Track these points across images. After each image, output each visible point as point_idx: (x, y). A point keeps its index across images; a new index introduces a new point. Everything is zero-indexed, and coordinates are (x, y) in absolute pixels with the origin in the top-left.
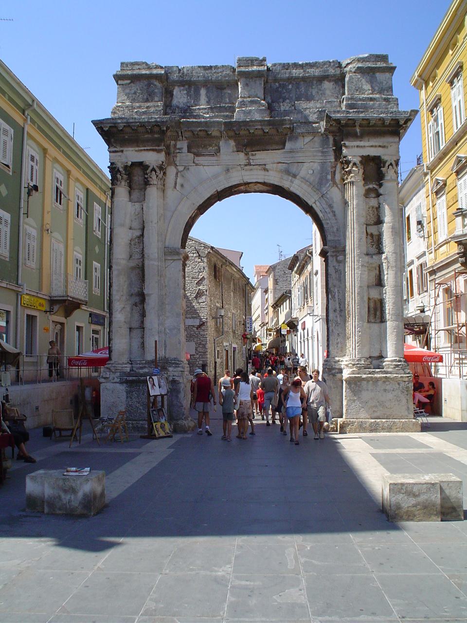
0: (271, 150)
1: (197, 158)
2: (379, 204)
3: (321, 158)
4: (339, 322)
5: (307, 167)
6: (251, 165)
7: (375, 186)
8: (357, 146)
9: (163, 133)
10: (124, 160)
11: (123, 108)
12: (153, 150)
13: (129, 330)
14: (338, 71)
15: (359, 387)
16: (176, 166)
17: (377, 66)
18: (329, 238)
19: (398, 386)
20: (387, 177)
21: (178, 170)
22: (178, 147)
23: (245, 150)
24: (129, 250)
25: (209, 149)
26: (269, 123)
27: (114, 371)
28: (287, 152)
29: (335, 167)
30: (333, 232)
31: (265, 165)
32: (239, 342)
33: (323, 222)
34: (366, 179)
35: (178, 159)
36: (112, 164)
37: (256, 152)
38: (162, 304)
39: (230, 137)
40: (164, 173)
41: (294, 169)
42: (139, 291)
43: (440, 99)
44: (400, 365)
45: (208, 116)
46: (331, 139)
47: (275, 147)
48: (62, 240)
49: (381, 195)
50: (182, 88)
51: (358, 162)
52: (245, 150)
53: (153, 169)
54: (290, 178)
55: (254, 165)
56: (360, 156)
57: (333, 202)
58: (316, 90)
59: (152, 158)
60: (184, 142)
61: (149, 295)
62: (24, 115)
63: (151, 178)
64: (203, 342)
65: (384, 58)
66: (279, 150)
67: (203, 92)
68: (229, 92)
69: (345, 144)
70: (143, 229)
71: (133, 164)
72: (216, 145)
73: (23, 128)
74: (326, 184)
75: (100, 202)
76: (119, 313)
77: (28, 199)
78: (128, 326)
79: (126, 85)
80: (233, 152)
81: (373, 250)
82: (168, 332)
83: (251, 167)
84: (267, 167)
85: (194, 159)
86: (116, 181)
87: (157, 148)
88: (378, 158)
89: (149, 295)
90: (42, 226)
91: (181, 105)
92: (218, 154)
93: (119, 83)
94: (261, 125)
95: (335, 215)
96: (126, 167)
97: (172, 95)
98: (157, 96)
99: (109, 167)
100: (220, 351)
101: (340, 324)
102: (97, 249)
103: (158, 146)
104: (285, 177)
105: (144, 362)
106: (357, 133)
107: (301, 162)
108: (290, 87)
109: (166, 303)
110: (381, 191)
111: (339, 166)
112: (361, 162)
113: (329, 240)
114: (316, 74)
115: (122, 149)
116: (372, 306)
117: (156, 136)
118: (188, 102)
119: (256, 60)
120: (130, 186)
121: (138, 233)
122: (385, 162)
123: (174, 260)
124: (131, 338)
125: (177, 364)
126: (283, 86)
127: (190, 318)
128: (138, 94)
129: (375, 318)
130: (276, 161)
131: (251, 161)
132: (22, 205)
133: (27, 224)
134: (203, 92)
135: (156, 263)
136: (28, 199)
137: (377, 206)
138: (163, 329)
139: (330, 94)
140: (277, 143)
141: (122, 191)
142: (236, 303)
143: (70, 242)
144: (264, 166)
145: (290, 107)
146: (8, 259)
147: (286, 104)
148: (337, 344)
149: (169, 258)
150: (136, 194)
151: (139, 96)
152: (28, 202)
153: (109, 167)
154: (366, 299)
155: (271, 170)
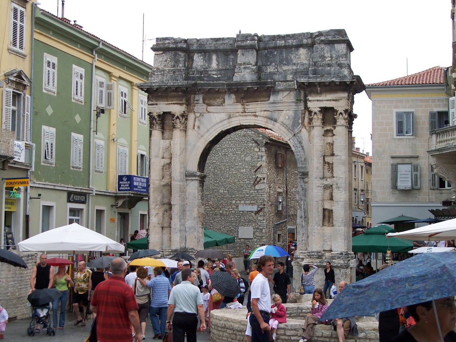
1: (209, 107)
2: (333, 141)
3: (295, 107)
4: (304, 225)
6: (246, 112)
7: (332, 128)
8: (317, 100)
10: (158, 111)
12: (178, 104)
13: (161, 228)
14: (310, 41)
16: (195, 113)
19: (339, 272)
20: (338, 123)
21: (196, 116)
23: (242, 101)
24: (161, 173)
26: (256, 84)
29: (305, 114)
30: (302, 161)
31: (256, 112)
34: (324, 122)
35: (196, 108)
37: (250, 103)
38: (183, 211)
39: (232, 93)
40: (186, 119)
41: (275, 115)
42: (168, 202)
44: (341, 257)
45: (216, 76)
46: (302, 93)
47: (263, 99)
48: (127, 143)
49: (334, 135)
50: (200, 54)
52: (242, 101)
53: (178, 117)
54: (273, 122)
55: (248, 113)
56: (319, 108)
57: (302, 140)
58: (294, 55)
59: (177, 109)
61: (174, 205)
63: (176, 123)
64: (260, 227)
65: (341, 33)
67: (214, 57)
68: (233, 57)
69: (308, 99)
70: (171, 158)
71: (164, 113)
72: (222, 98)
73: (92, 64)
74: (297, 126)
76: (154, 217)
77: (97, 119)
78: (161, 225)
79: (160, 54)
80: (234, 103)
81: (328, 174)
83: (246, 114)
84: (257, 114)
85: (207, 107)
86: (152, 125)
88: (333, 108)
89: (174, 205)
90: (109, 137)
91: (199, 68)
92: (223, 104)
95: (303, 149)
96: (159, 116)
97: (193, 60)
98: (181, 64)
103: (181, 101)
104: (269, 121)
105: (170, 251)
108: (276, 53)
109: (187, 210)
110: (334, 132)
111: (307, 113)
112: (319, 111)
113: (299, 167)
114: (294, 44)
117: (180, 93)
118: (204, 65)
119: (250, 36)
121: (167, 161)
123: (193, 180)
124: (163, 234)
126: (271, 53)
128: (168, 62)
129: (329, 223)
130: (263, 109)
131: (246, 110)
132: (92, 126)
133: (97, 138)
134: (214, 57)
135: (179, 183)
136: (97, 119)
139: (304, 58)
140: (264, 97)
141: (157, 133)
143: (135, 144)
144: (255, 113)
146: (81, 170)
147: (271, 67)
148: (302, 240)
149: (190, 179)
150: (167, 134)
151: (168, 63)
152: (97, 121)
155: (259, 116)
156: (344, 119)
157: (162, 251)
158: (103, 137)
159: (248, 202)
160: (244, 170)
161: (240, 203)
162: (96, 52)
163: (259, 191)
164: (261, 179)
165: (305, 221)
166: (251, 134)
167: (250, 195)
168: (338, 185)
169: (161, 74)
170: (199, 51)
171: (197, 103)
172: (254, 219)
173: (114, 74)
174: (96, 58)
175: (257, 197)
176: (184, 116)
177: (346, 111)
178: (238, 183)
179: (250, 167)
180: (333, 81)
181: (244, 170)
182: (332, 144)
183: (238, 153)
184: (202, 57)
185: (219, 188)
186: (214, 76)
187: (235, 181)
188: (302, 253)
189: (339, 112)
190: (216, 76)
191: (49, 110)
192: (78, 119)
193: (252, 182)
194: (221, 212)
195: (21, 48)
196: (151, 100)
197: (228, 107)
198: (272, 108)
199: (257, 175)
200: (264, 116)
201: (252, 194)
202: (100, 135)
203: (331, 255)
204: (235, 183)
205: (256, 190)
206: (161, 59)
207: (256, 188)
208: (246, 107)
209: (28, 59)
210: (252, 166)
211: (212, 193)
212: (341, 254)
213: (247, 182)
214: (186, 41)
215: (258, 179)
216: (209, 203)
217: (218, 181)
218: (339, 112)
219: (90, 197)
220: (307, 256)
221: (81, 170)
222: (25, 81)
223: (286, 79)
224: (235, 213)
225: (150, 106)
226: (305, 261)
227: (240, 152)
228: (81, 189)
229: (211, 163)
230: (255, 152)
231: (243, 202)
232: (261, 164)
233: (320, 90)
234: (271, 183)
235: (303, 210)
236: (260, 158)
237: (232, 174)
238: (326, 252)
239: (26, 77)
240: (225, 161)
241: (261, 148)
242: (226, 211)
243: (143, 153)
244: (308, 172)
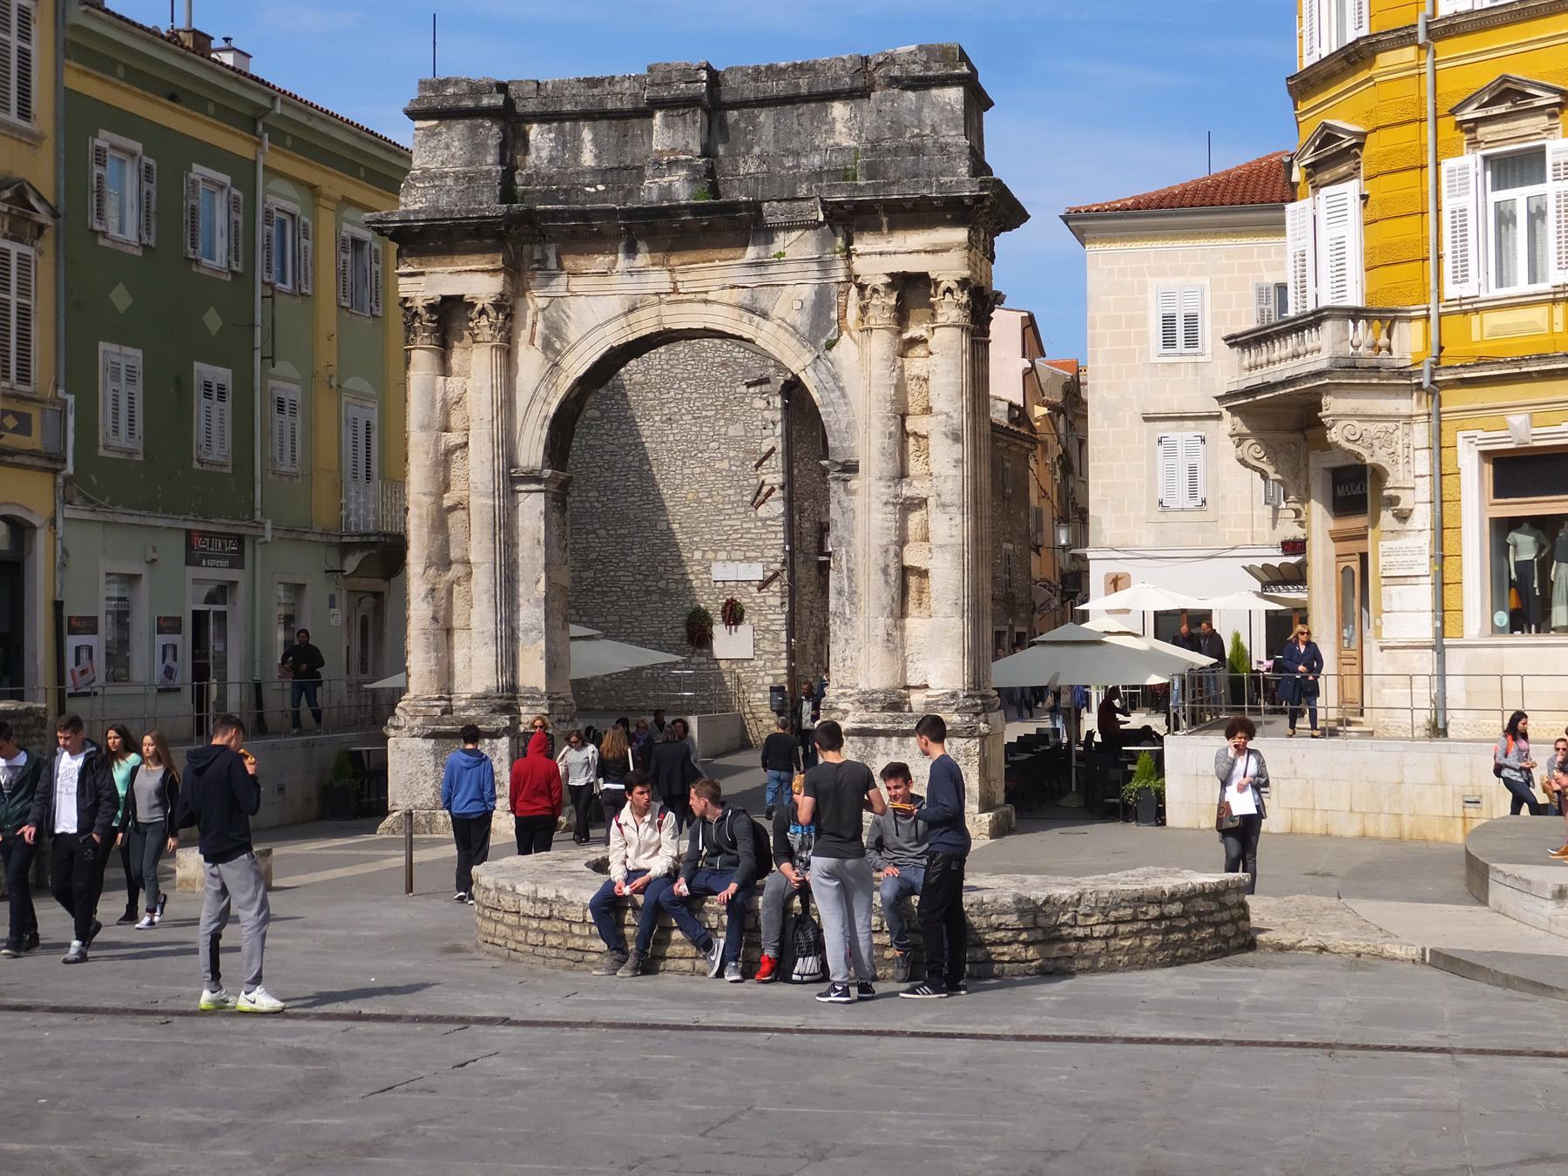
0: (720, 260)
1: (574, 281)
3: (818, 275)
5: (790, 295)
8: (881, 254)
12: (483, 271)
13: (445, 634)
15: (872, 748)
17: (930, 73)
20: (941, 320)
22: (536, 257)
23: (668, 260)
28: (750, 265)
31: (706, 292)
34: (901, 316)
39: (641, 237)
44: (953, 704)
45: (593, 190)
49: (931, 353)
50: (546, 126)
53: (483, 312)
54: (757, 318)
56: (887, 275)
60: (547, 246)
62: (255, 134)
66: (735, 259)
67: (587, 135)
71: (445, 299)
73: (255, 163)
84: (710, 297)
88: (925, 275)
94: (691, 214)
95: (844, 396)
96: (431, 308)
101: (850, 619)
107: (778, 285)
108: (762, 118)
111: (854, 290)
112: (888, 285)
117: (489, 241)
122: (937, 284)
123: (530, 492)
125: (537, 699)
126: (752, 120)
127: (741, 561)
128: (453, 149)
133: (276, 377)
134: (587, 135)
139: (844, 130)
144: (704, 296)
145: (758, 167)
146: (229, 470)
154: (892, 571)
156: (959, 305)
158: (296, 375)
159: (739, 555)
160: (725, 464)
161: (715, 560)
162: (267, 128)
163: (768, 522)
164: (773, 490)
165: (852, 603)
166: (744, 358)
167: (742, 534)
168: (943, 497)
169: (434, 186)
170: (544, 118)
171: (538, 269)
172: (755, 603)
173: (325, 190)
174: (266, 142)
175: (764, 539)
176: (507, 308)
177: (963, 283)
178: (709, 500)
179: (741, 455)
180: (923, 197)
181: (726, 461)
182: (926, 380)
183: (709, 414)
184: (552, 135)
185: (656, 518)
186: (588, 189)
187: (701, 495)
188: (843, 694)
189: (943, 286)
190: (593, 190)
191: (121, 298)
192: (213, 321)
193: (749, 498)
194: (662, 584)
195: (25, 113)
196: (405, 263)
197: (628, 278)
198: (753, 279)
199: (763, 478)
200: (731, 302)
201: (747, 533)
202: (283, 367)
203: (925, 700)
204: (699, 501)
205: (761, 519)
206: (432, 143)
207: (760, 515)
208: (679, 277)
209: (48, 147)
210: (746, 451)
211: (635, 530)
212: (954, 695)
213: (732, 498)
214: (502, 88)
215: (765, 489)
216: (628, 559)
217: (651, 497)
218: (943, 286)
219: (258, 548)
220: (857, 704)
221: (229, 470)
222: (38, 212)
223: (796, 192)
224: (702, 586)
226: (850, 718)
227: (713, 413)
228: (228, 525)
229: (630, 445)
230: (756, 409)
231: (722, 555)
232: (772, 444)
234: (806, 500)
236: (771, 426)
237: (693, 474)
238: (911, 691)
239: (41, 198)
240: (671, 438)
241: (771, 400)
242: (675, 581)
244: (858, 462)
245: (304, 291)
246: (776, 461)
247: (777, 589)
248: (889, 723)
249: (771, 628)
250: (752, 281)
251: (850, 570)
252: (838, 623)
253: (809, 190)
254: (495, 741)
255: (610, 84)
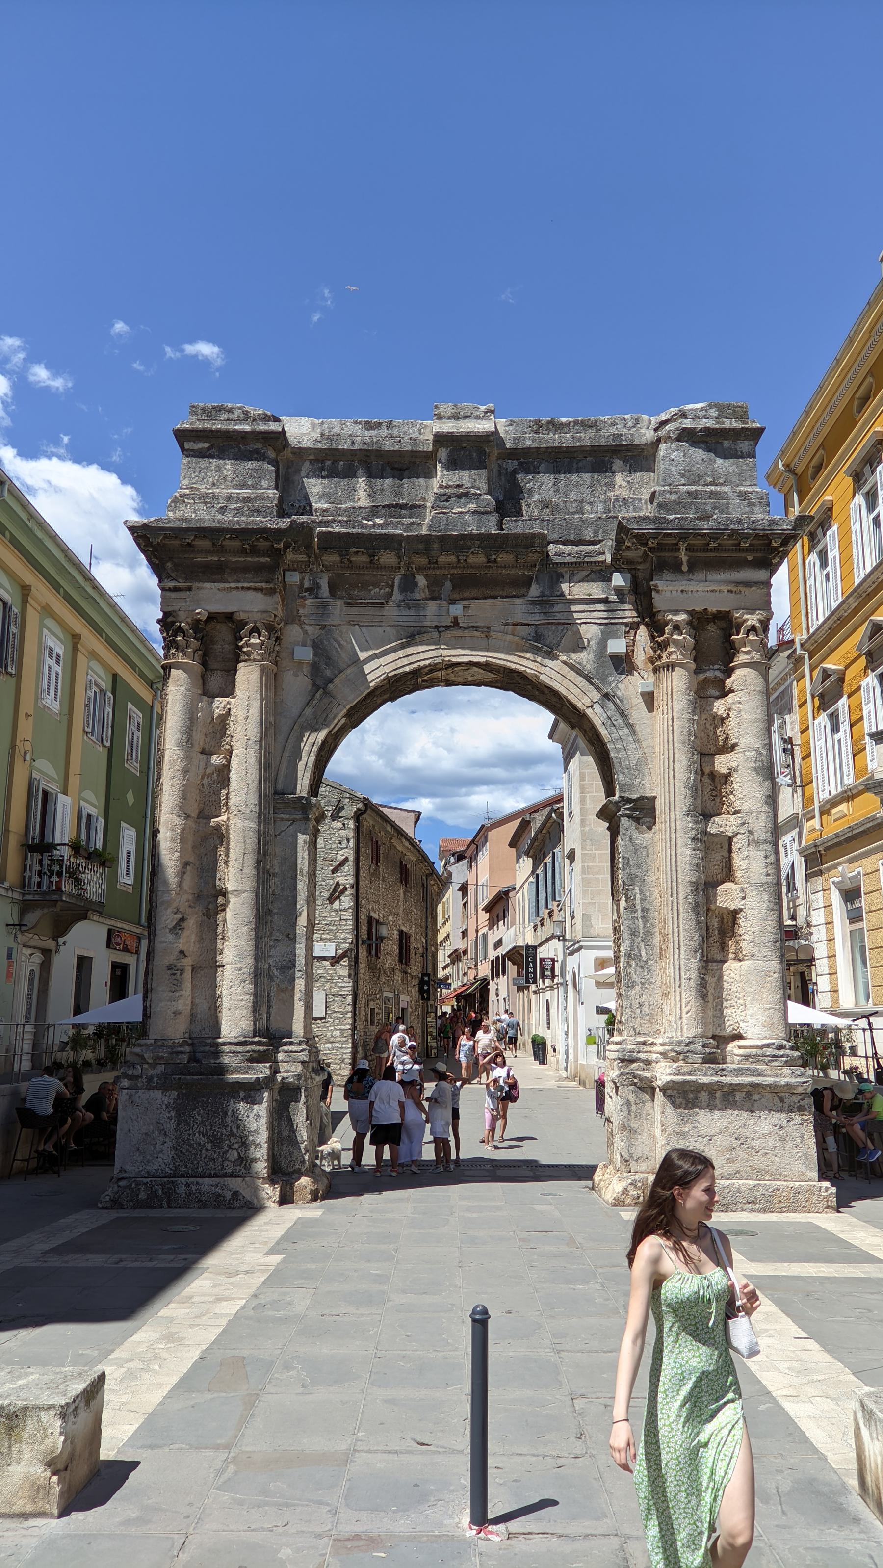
0: (502, 597)
4: (644, 959)
9: (277, 555)
11: (193, 499)
12: (255, 589)
16: (301, 624)
18: (620, 777)
20: (742, 658)
22: (306, 585)
25: (372, 592)
27: (150, 1061)
28: (534, 603)
32: (413, 990)
33: (610, 746)
36: (166, 614)
39: (419, 569)
43: (830, 509)
44: (782, 1056)
45: (371, 523)
48: (56, 777)
51: (683, 625)
66: (518, 597)
69: (656, 586)
71: (212, 617)
72: (387, 585)
75: (139, 702)
82: (276, 973)
87: (264, 585)
93: (186, 447)
95: (633, 733)
96: (196, 625)
99: (159, 621)
100: (377, 1011)
101: (646, 962)
102: (130, 798)
106: (682, 563)
107: (563, 624)
109: (275, 911)
112: (690, 623)
115: (189, 584)
116: (716, 925)
120: (204, 664)
128: (225, 472)
137: (724, 715)
138: (266, 967)
142: (408, 913)
148: (641, 1005)
153: (159, 621)
157: (190, 1041)
163: (342, 913)
188: (644, 1043)
198: (537, 617)
199: (338, 879)
205: (335, 911)
225: (168, 594)
232: (346, 854)
233: (688, 561)
235: (639, 911)
243: (94, 811)
245: (10, 670)
246: (349, 868)
247: (346, 963)
248: (712, 1075)
249: (341, 993)
250: (537, 619)
251: (645, 910)
252: (633, 966)
253: (596, 533)
254: (252, 1093)
255: (388, 427)
